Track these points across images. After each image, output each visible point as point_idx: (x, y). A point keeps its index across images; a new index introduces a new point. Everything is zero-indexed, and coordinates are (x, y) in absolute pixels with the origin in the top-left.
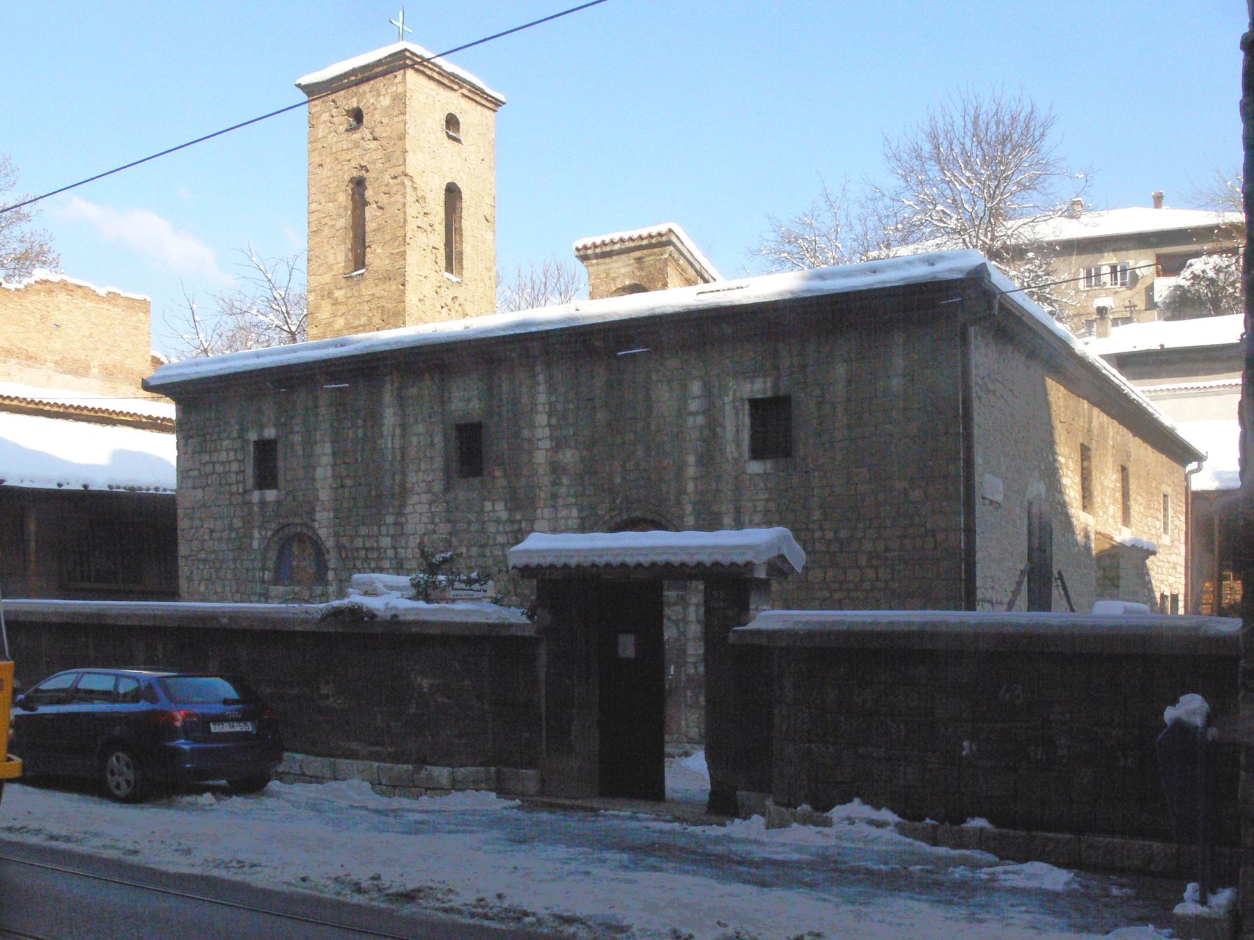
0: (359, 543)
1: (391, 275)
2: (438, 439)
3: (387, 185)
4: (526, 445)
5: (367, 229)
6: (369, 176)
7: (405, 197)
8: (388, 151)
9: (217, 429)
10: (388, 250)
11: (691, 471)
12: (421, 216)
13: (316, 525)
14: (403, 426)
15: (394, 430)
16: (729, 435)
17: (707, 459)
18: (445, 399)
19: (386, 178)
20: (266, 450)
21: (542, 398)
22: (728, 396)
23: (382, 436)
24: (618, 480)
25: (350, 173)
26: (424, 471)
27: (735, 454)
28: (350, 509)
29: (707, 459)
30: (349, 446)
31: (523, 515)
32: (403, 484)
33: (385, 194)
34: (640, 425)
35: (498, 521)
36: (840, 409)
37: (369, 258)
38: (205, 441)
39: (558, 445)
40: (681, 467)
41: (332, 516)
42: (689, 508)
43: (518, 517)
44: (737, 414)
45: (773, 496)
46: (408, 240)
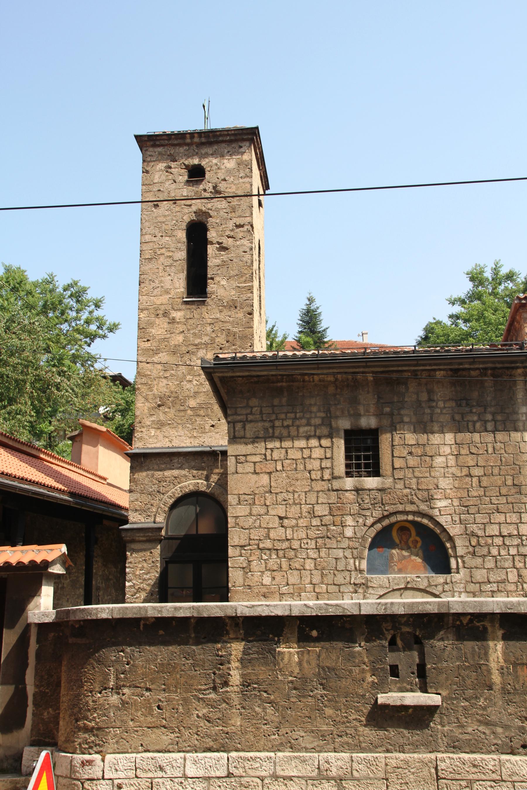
0: (493, 530)
1: (238, 305)
3: (232, 230)
5: (209, 264)
7: (252, 243)
8: (232, 203)
9: (292, 415)
10: (235, 284)
13: (436, 512)
19: (231, 225)
33: (229, 237)
37: (211, 287)
41: (456, 503)
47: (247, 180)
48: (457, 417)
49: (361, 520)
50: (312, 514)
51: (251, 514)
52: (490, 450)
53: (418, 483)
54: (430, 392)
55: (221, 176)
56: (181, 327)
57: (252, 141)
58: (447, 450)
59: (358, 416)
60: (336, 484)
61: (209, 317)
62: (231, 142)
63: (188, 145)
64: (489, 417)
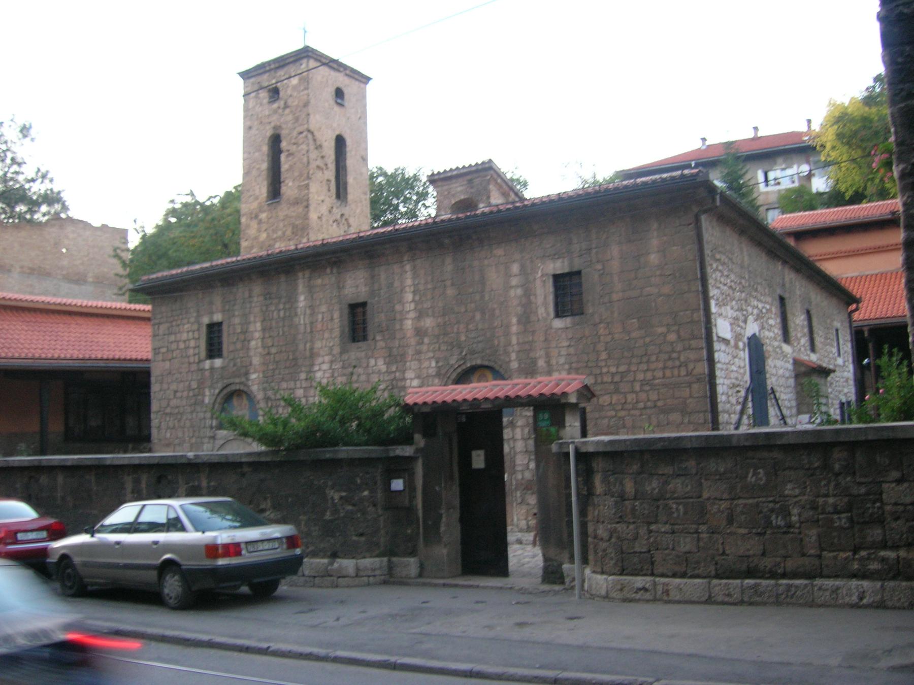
2: (336, 315)
4: (398, 317)
5: (283, 170)
6: (284, 133)
9: (181, 317)
11: (514, 329)
12: (319, 159)
13: (250, 383)
14: (311, 307)
15: (305, 311)
16: (540, 300)
17: (526, 319)
18: (341, 286)
19: (295, 133)
20: (214, 330)
21: (409, 282)
22: (537, 273)
23: (296, 315)
24: (463, 338)
25: (269, 133)
26: (327, 340)
27: (544, 315)
28: (274, 370)
29: (526, 319)
30: (274, 323)
31: (397, 368)
32: (312, 349)
34: (478, 297)
35: (379, 372)
36: (616, 278)
37: (284, 189)
38: (172, 326)
39: (421, 315)
40: (508, 326)
41: (261, 375)
42: (513, 356)
43: (394, 369)
44: (544, 286)
45: (572, 344)
46: (310, 176)
47: (306, 92)
48: (264, 308)
49: (212, 391)
50: (190, 389)
51: (161, 390)
52: (281, 333)
53: (241, 362)
54: (250, 291)
55: (289, 92)
56: (264, 226)
57: (308, 57)
58: (257, 335)
59: (212, 313)
60: (201, 366)
61: (281, 214)
62: (295, 62)
63: (270, 70)
64: (281, 306)
